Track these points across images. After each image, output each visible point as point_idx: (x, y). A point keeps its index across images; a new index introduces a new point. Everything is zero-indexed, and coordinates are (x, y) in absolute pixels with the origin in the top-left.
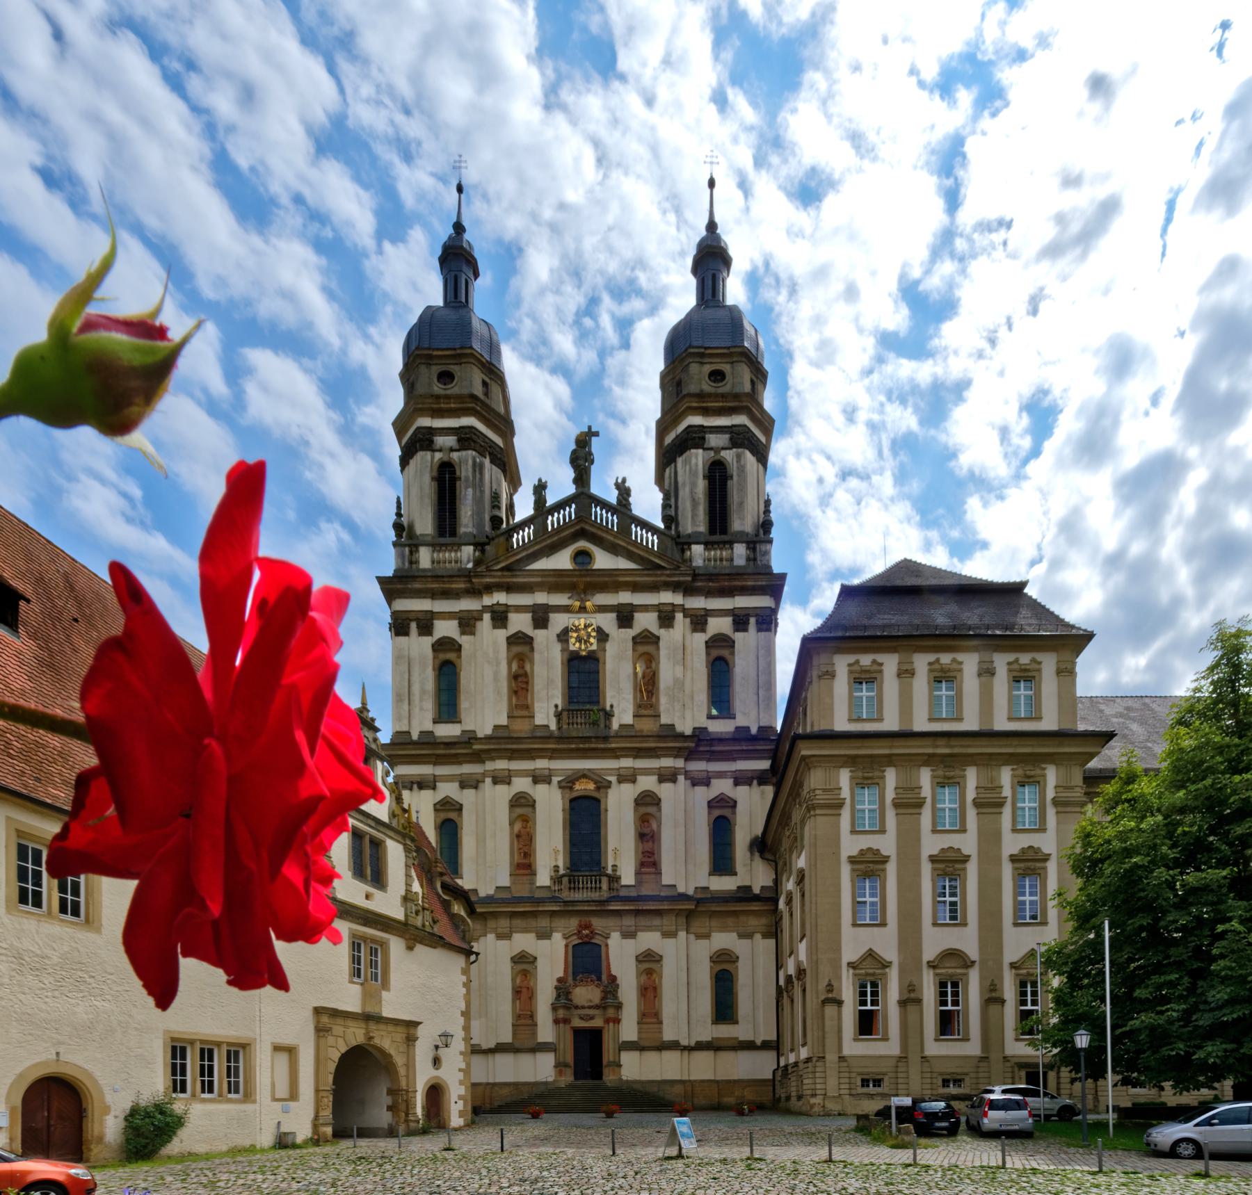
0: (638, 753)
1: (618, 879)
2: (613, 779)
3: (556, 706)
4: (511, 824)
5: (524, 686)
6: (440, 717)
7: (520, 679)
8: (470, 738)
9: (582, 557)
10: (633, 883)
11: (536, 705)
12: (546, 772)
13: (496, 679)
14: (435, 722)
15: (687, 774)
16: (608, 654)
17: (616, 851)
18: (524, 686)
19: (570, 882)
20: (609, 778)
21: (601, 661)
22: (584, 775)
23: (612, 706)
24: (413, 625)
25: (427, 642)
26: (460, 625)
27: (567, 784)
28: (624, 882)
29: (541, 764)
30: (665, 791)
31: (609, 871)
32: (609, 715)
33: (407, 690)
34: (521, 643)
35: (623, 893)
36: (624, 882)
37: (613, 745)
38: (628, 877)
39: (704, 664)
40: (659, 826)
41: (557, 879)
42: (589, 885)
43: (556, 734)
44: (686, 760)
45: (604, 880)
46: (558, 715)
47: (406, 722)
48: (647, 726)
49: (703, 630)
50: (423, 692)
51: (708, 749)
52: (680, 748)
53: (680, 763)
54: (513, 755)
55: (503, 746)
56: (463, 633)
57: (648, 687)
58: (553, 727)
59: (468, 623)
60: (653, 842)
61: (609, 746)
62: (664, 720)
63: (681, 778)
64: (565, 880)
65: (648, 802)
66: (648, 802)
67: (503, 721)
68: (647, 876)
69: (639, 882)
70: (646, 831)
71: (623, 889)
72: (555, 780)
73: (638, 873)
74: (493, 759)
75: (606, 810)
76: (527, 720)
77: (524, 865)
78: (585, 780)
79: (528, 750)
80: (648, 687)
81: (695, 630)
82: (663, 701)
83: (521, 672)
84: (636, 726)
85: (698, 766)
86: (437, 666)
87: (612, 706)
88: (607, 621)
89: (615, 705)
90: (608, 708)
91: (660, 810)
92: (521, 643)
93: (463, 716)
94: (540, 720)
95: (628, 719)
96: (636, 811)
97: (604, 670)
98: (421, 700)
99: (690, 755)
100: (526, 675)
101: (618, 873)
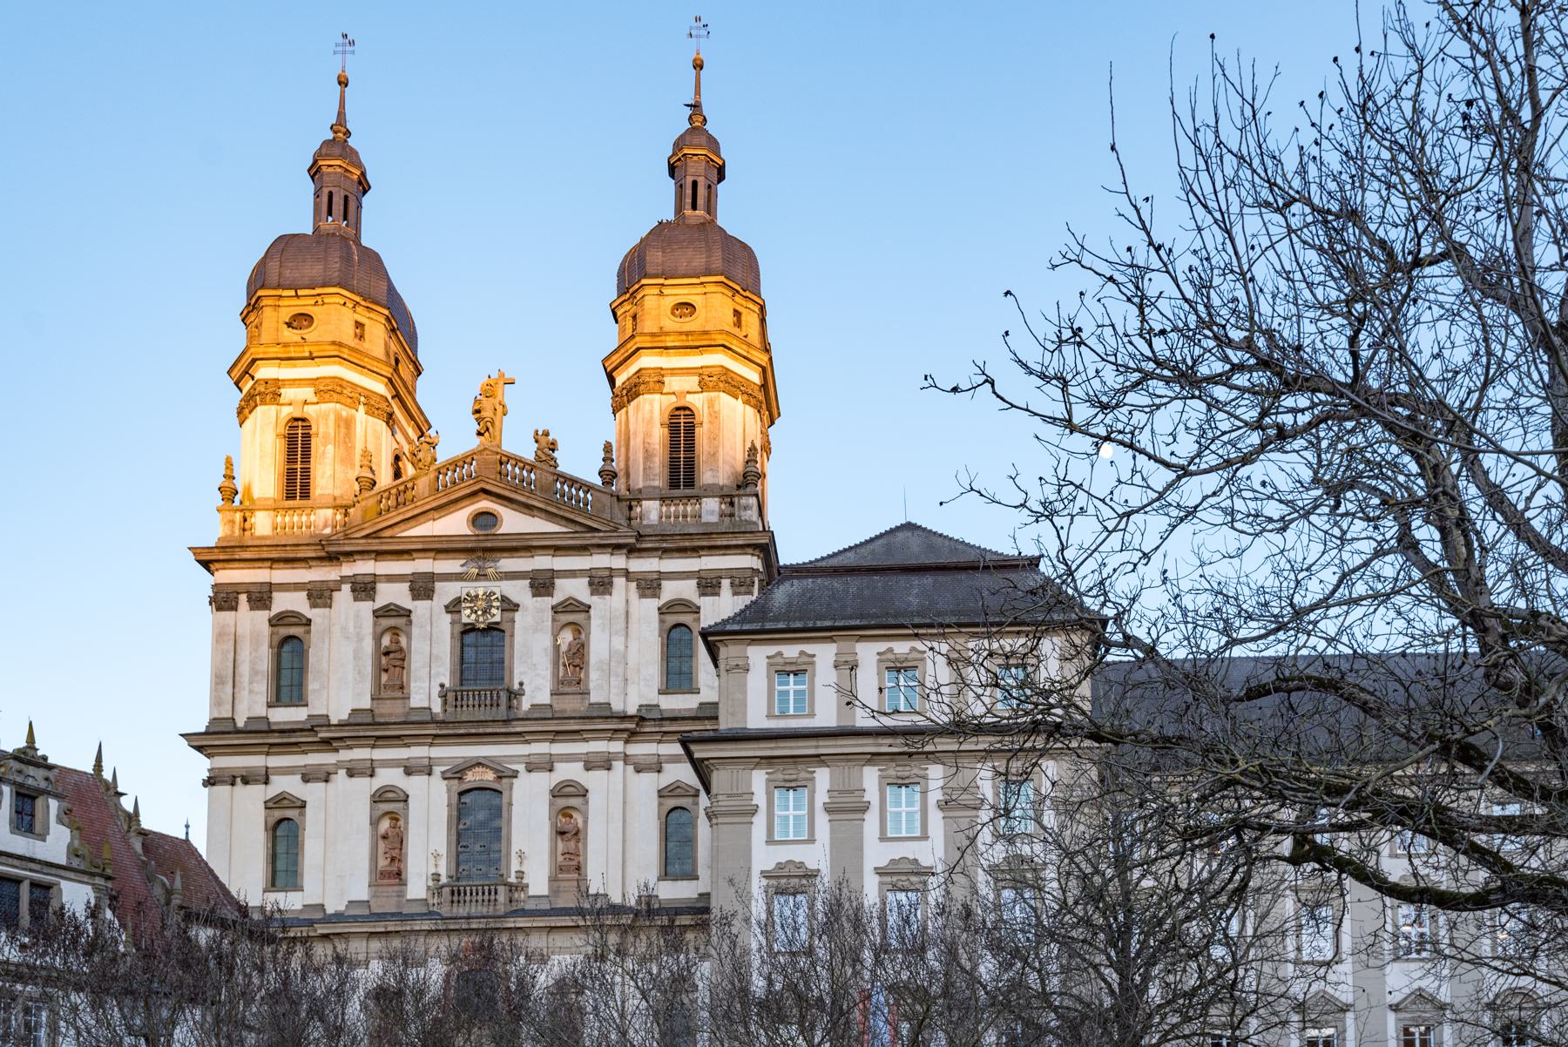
0: (557, 736)
1: (524, 888)
2: (521, 768)
3: (442, 686)
4: (374, 823)
5: (398, 663)
6: (278, 700)
7: (392, 655)
8: (316, 725)
9: (484, 520)
10: (546, 892)
11: (412, 685)
12: (426, 762)
13: (357, 655)
14: (269, 706)
15: (626, 759)
16: (517, 625)
17: (521, 855)
18: (398, 663)
19: (453, 893)
20: (514, 767)
21: (507, 634)
22: (478, 763)
23: (521, 684)
24: (243, 598)
25: (263, 616)
26: (309, 596)
27: (456, 773)
28: (532, 891)
29: (418, 752)
30: (594, 781)
31: (512, 879)
32: (519, 694)
33: (231, 671)
34: (393, 619)
35: (530, 906)
36: (532, 891)
37: (519, 729)
38: (538, 883)
39: (656, 633)
40: (586, 822)
41: (437, 890)
42: (480, 898)
43: (441, 717)
44: (627, 742)
45: (501, 889)
46: (444, 696)
47: (229, 707)
48: (571, 705)
49: (656, 596)
50: (254, 672)
51: (657, 729)
52: (616, 731)
53: (617, 746)
54: (378, 741)
55: (362, 734)
56: (314, 606)
57: (573, 662)
58: (437, 708)
59: (320, 595)
60: (578, 841)
61: (512, 730)
62: (595, 697)
63: (618, 765)
64: (446, 891)
65: (568, 800)
66: (568, 800)
67: (366, 703)
68: (566, 884)
69: (554, 893)
70: (566, 828)
71: (532, 900)
72: (437, 770)
73: (553, 879)
74: (350, 747)
75: (510, 804)
76: (400, 701)
77: (391, 872)
78: (481, 769)
79: (398, 737)
80: (573, 662)
81: (642, 596)
82: (594, 677)
83: (393, 647)
84: (555, 706)
85: (639, 749)
86: (275, 643)
87: (521, 684)
88: (518, 591)
89: (526, 682)
90: (516, 686)
91: (587, 802)
92: (393, 619)
93: (311, 698)
94: (417, 700)
95: (544, 697)
96: (551, 804)
97: (512, 646)
98: (251, 682)
99: (632, 736)
100: (401, 650)
101: (525, 881)
